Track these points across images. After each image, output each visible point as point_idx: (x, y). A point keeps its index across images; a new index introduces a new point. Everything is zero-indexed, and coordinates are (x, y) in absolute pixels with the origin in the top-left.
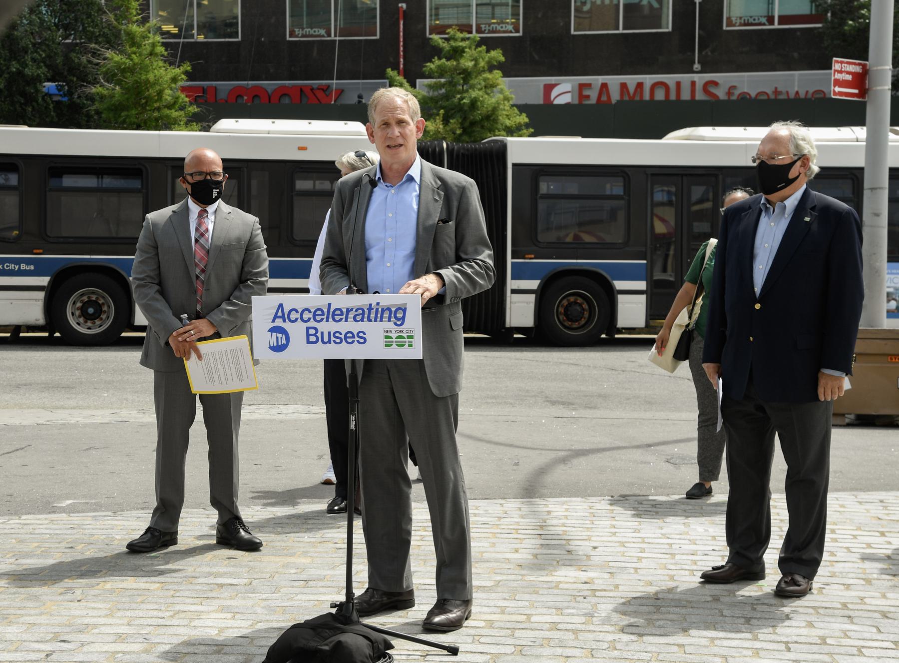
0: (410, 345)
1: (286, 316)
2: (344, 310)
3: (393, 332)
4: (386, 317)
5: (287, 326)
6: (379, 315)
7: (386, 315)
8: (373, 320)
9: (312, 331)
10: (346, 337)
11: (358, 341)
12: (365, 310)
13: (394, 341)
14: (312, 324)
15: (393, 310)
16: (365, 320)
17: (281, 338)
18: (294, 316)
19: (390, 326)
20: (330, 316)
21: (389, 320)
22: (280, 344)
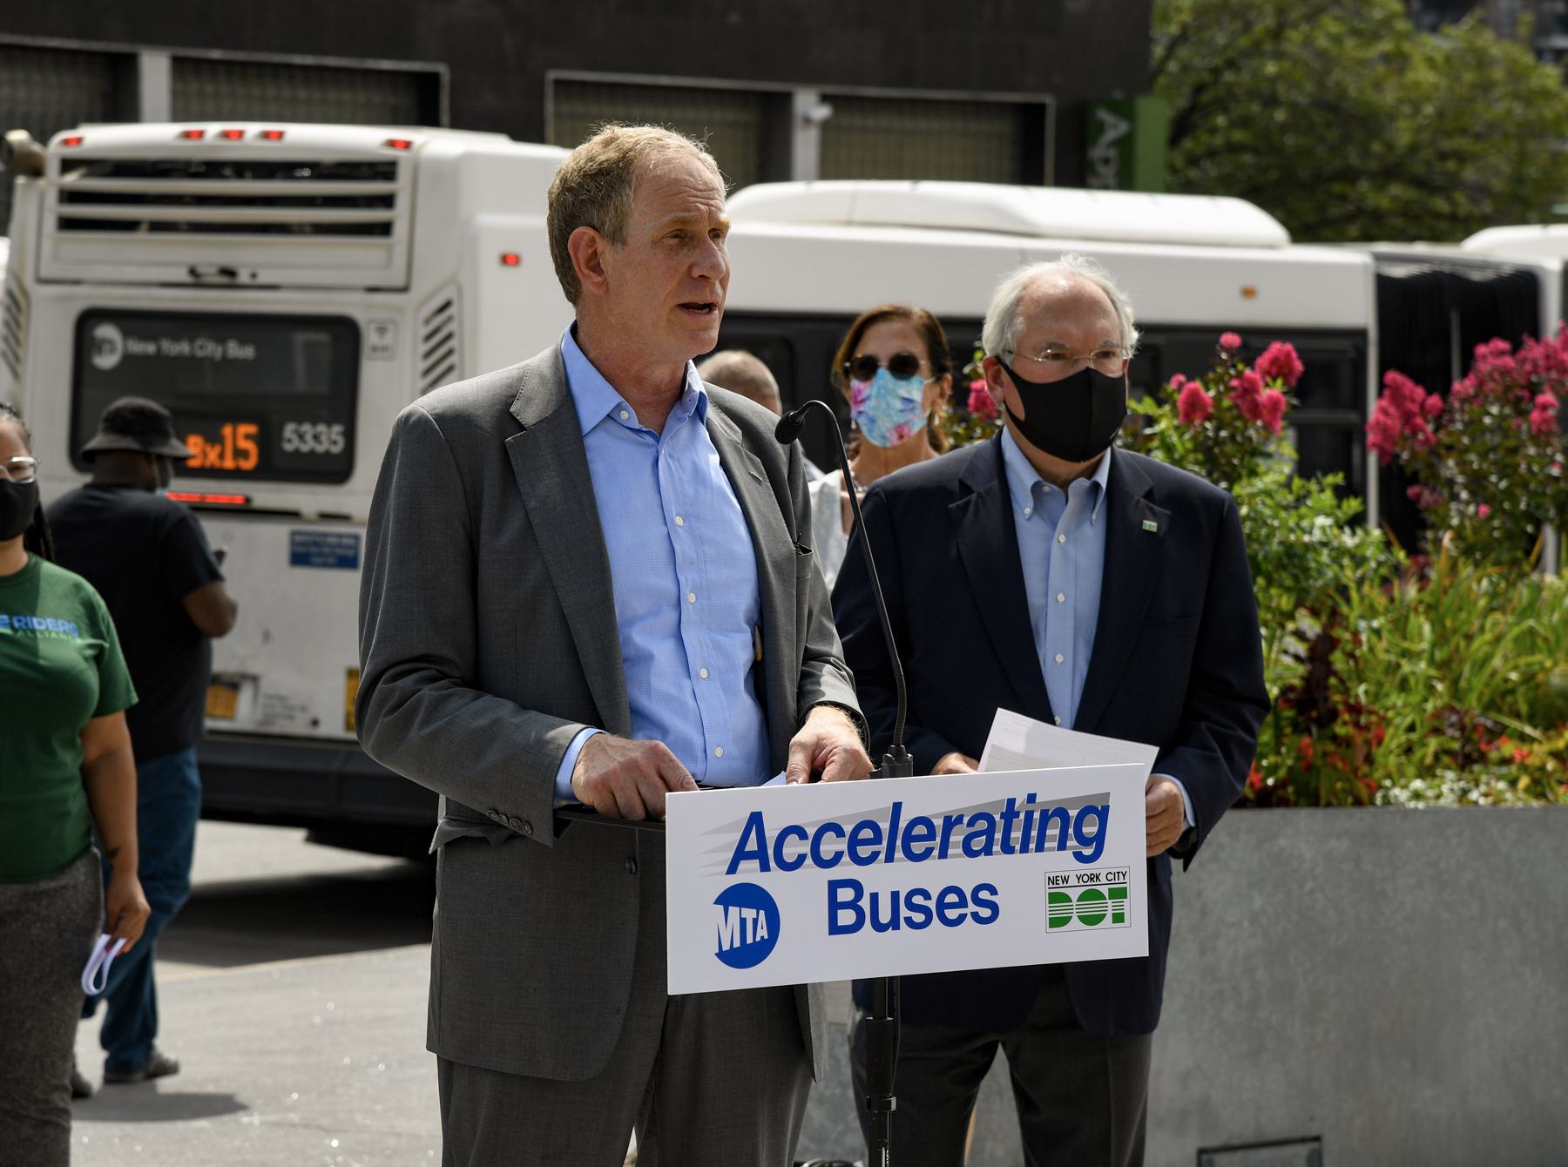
0: (1118, 918)
1: (770, 852)
2: (938, 823)
3: (1073, 881)
4: (1052, 838)
5: (773, 882)
6: (1034, 833)
7: (1053, 831)
8: (1018, 847)
9: (845, 895)
10: (942, 905)
11: (975, 916)
12: (997, 817)
13: (1075, 909)
14: (846, 870)
15: (1073, 813)
16: (997, 848)
17: (755, 921)
18: (793, 848)
19: (1062, 862)
20: (899, 843)
22: (749, 940)
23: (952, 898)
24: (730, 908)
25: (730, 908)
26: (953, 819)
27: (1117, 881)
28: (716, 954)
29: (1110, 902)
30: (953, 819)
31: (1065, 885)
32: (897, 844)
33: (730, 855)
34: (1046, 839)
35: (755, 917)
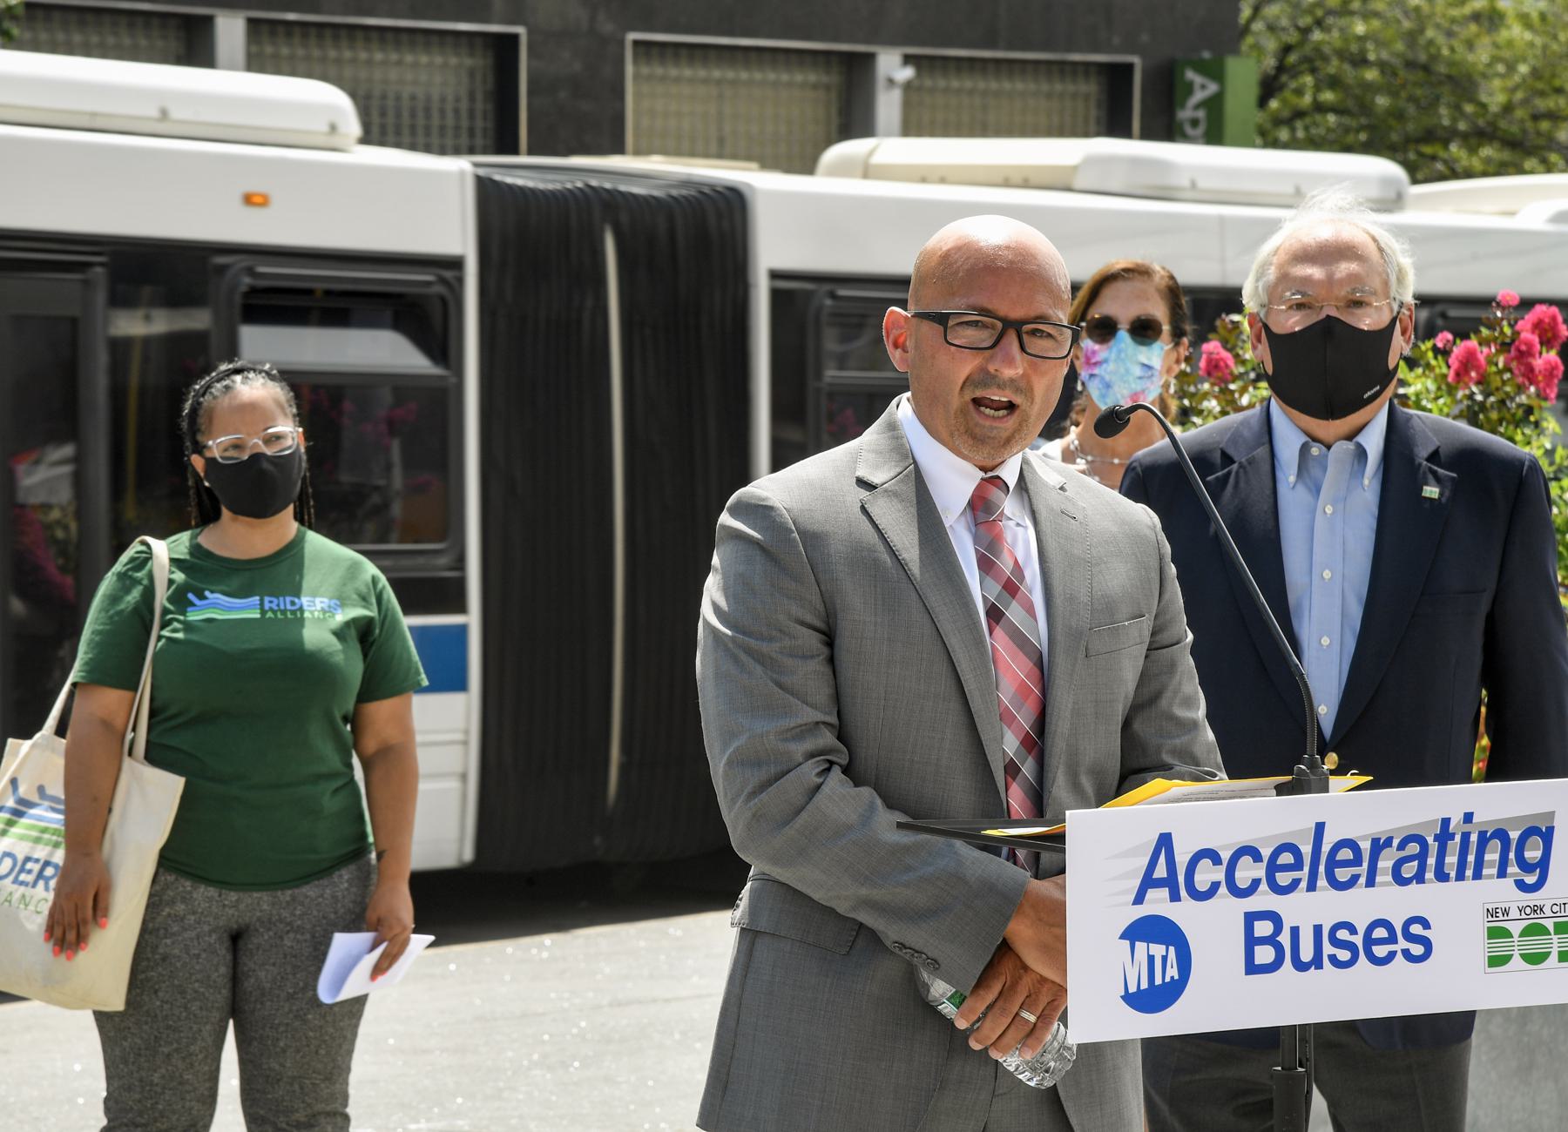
1: (1181, 879)
2: (1366, 846)
4: (1491, 866)
5: (1184, 914)
6: (1471, 858)
7: (1492, 856)
8: (1453, 874)
11: (1407, 954)
12: (1430, 840)
14: (1264, 900)
15: (1514, 835)
16: (1430, 875)
17: (1165, 959)
18: (1207, 875)
19: (1501, 891)
20: (1322, 869)
21: (1502, 873)
22: (1158, 981)
23: (1380, 933)
24: (1137, 943)
25: (1137, 943)
26: (1382, 841)
27: (1563, 914)
28: (1121, 997)
29: (1555, 938)
30: (1382, 841)
31: (1506, 918)
32: (1320, 870)
33: (1137, 882)
34: (1485, 864)
35: (1165, 954)
